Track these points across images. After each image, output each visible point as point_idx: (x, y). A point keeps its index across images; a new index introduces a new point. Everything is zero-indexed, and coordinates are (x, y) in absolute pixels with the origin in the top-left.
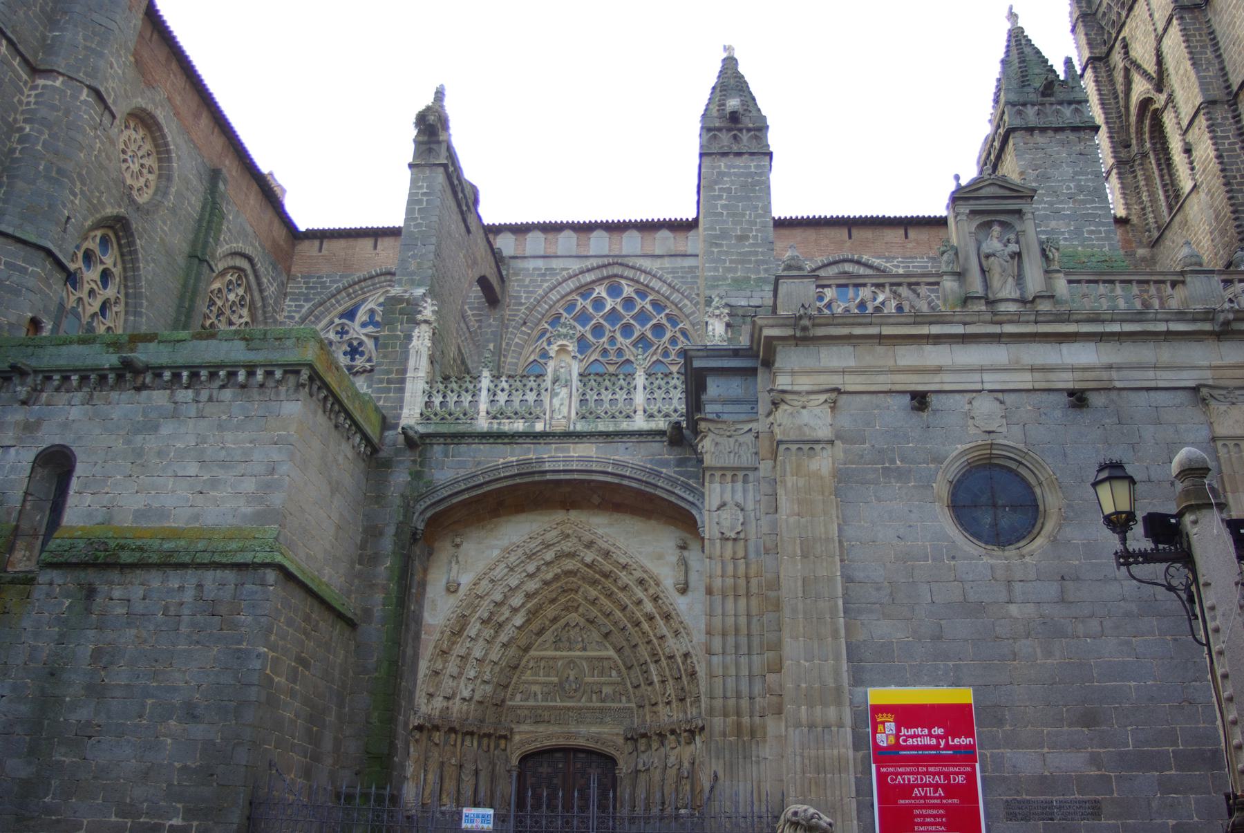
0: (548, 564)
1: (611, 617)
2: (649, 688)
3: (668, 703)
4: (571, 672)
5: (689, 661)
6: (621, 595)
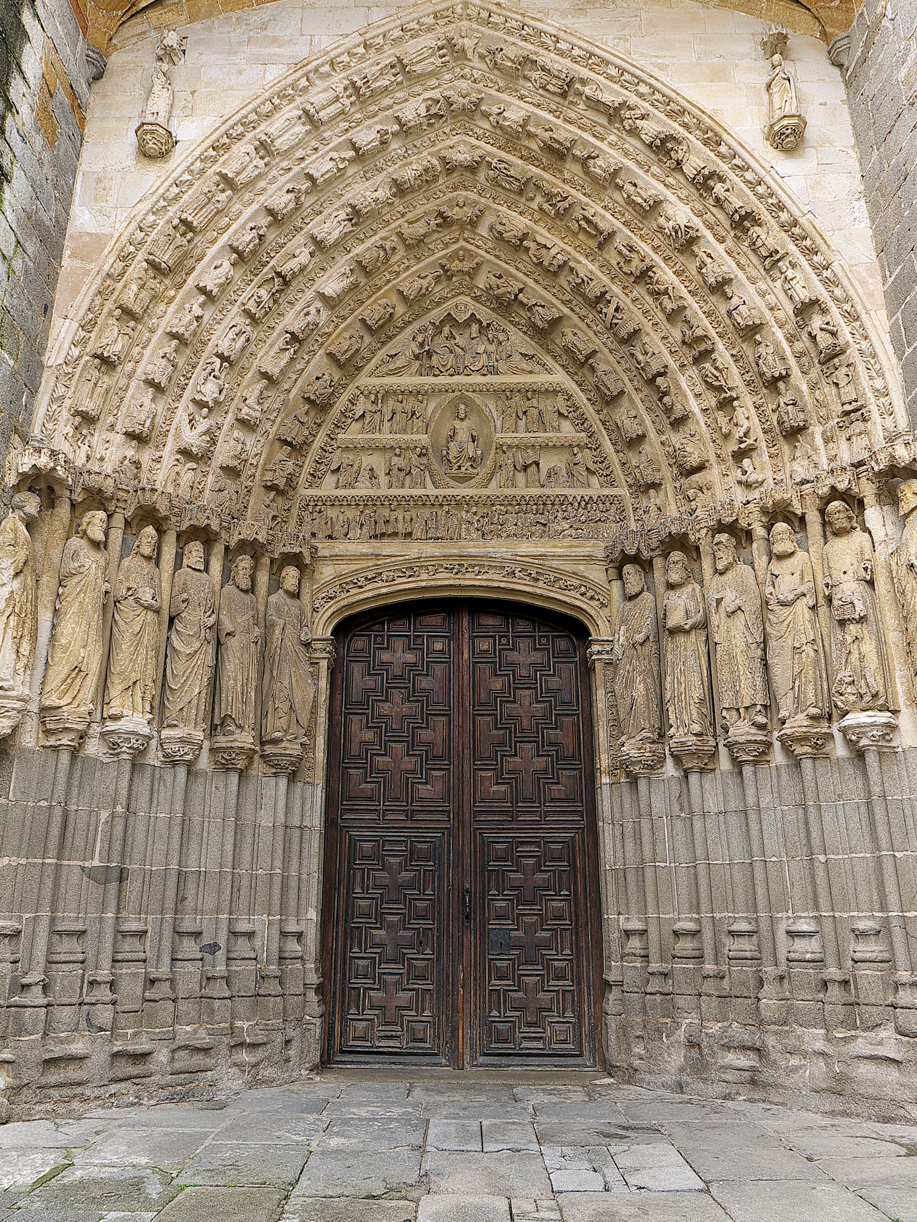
0: (405, 130)
1: (563, 281)
2: (676, 439)
3: (740, 455)
4: (458, 424)
5: (817, 322)
6: (594, 208)
